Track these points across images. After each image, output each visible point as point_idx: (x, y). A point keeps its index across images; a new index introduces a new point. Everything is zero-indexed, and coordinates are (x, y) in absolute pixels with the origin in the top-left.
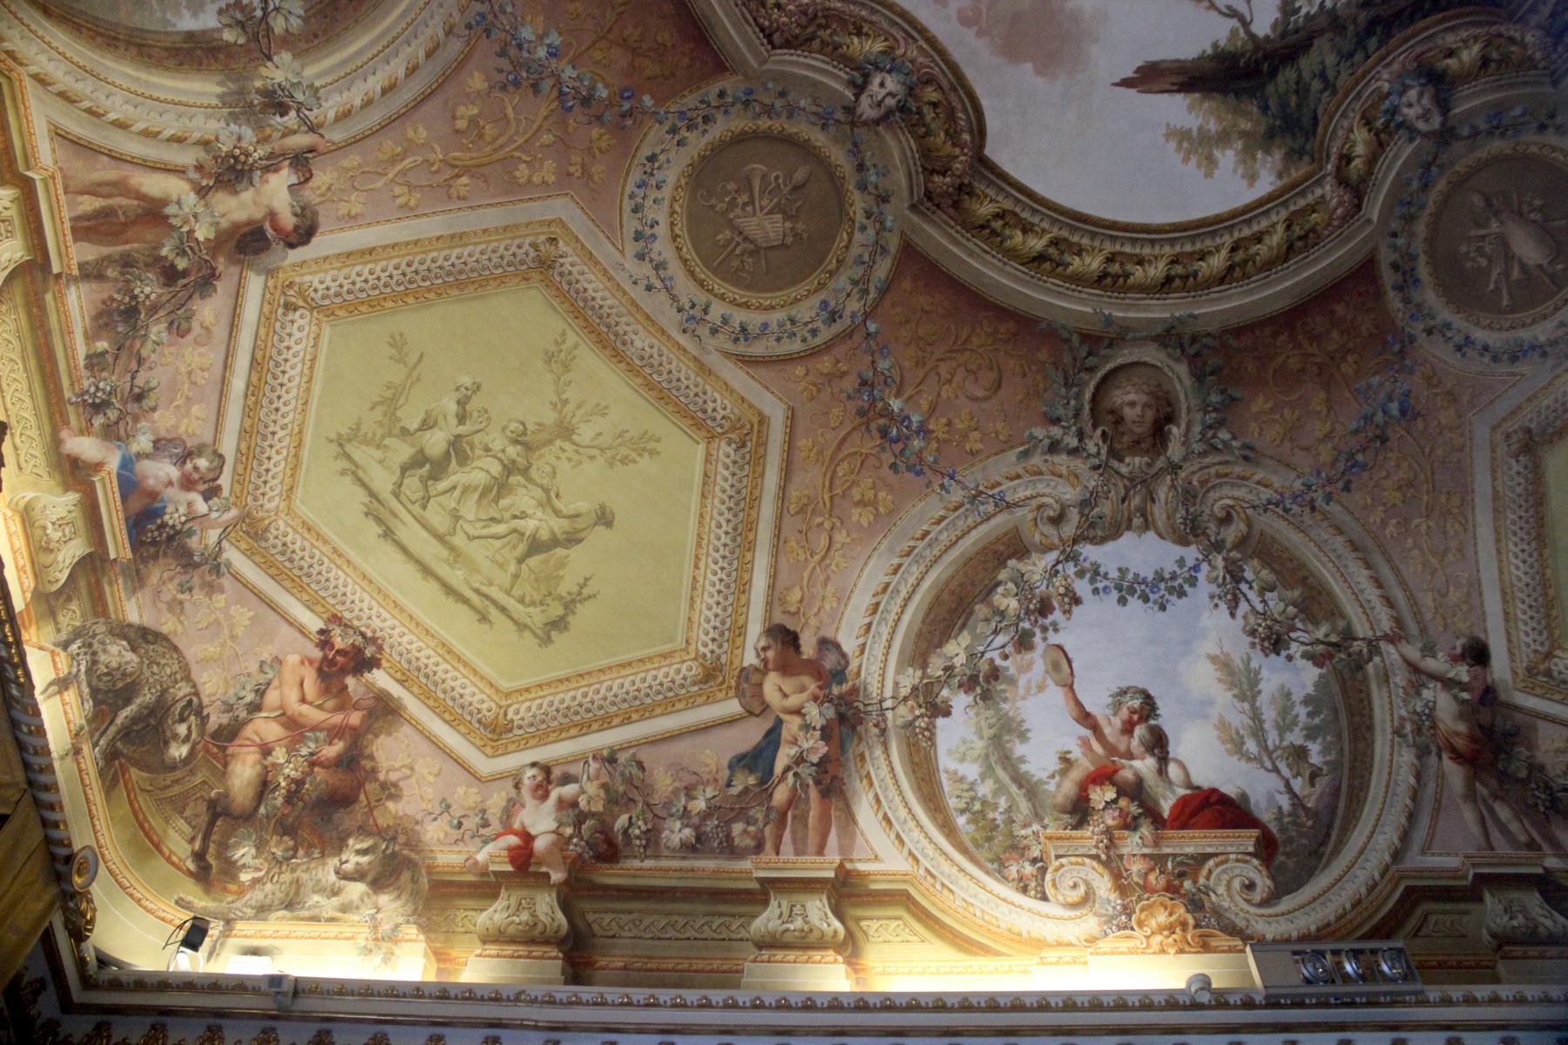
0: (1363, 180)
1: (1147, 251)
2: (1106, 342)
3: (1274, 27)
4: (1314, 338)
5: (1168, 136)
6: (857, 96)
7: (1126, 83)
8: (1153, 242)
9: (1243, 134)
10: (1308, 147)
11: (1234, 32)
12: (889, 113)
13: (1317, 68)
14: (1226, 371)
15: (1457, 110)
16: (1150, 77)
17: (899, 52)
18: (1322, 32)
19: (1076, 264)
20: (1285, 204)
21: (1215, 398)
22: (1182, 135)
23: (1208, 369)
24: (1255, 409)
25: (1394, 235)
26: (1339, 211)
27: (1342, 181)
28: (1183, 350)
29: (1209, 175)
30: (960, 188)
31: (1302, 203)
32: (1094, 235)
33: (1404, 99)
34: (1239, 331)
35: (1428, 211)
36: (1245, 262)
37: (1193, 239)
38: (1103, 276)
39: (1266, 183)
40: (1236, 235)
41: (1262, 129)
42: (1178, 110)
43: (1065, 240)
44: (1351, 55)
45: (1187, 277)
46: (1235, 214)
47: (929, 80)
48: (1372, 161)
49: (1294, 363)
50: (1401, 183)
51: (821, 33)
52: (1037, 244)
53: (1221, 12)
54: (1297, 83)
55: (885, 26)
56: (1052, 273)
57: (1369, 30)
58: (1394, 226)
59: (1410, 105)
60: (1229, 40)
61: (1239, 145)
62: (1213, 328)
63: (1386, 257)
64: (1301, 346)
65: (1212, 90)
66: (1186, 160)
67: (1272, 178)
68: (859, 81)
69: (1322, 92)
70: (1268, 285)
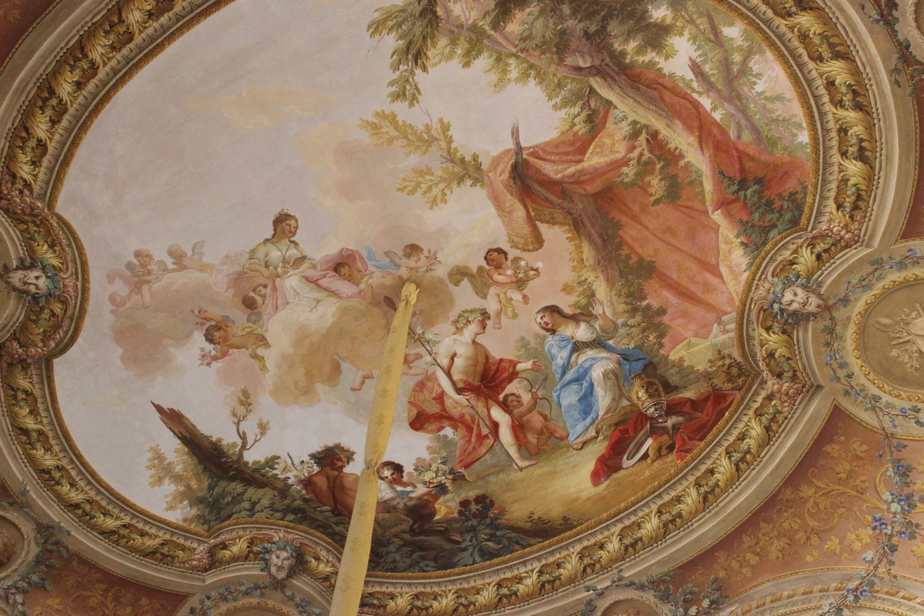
0: (221, 562)
1: (82, 484)
2: (11, 500)
3: (255, 463)
4: (116, 599)
5: (151, 449)
6: (18, 268)
7: (159, 409)
8: (89, 483)
9: (188, 487)
10: (212, 523)
11: (234, 445)
12: (27, 292)
13: (254, 499)
14: (55, 572)
15: (294, 582)
16: (173, 418)
17: (62, 275)
18: (274, 488)
19: (39, 453)
20: (173, 534)
21: (35, 578)
22: (159, 457)
23: (47, 562)
24: (49, 602)
25: (209, 598)
26: (195, 563)
27: (212, 552)
28: (45, 542)
29: (152, 485)
30: (22, 361)
31: (182, 541)
32: (63, 450)
33: (278, 552)
34: (82, 561)
35: (236, 604)
36: (124, 537)
37: (110, 502)
38: (48, 472)
39: (175, 516)
40: (134, 522)
41: (200, 494)
42: (171, 446)
43: (47, 437)
44: (276, 511)
45: (87, 515)
46: (143, 513)
47: (65, 302)
48: (235, 559)
49: (93, 602)
50: (238, 581)
51: (31, 226)
52: (30, 423)
53: (238, 431)
54: (238, 495)
55: (69, 258)
56: (22, 444)
57: (295, 511)
58: (213, 594)
59: (278, 557)
60: (228, 445)
61: (181, 489)
62: (73, 548)
63: (194, 602)
64: (106, 597)
65: (195, 454)
66: (148, 468)
67: (180, 518)
68: (28, 262)
69: (245, 510)
70: (122, 557)
